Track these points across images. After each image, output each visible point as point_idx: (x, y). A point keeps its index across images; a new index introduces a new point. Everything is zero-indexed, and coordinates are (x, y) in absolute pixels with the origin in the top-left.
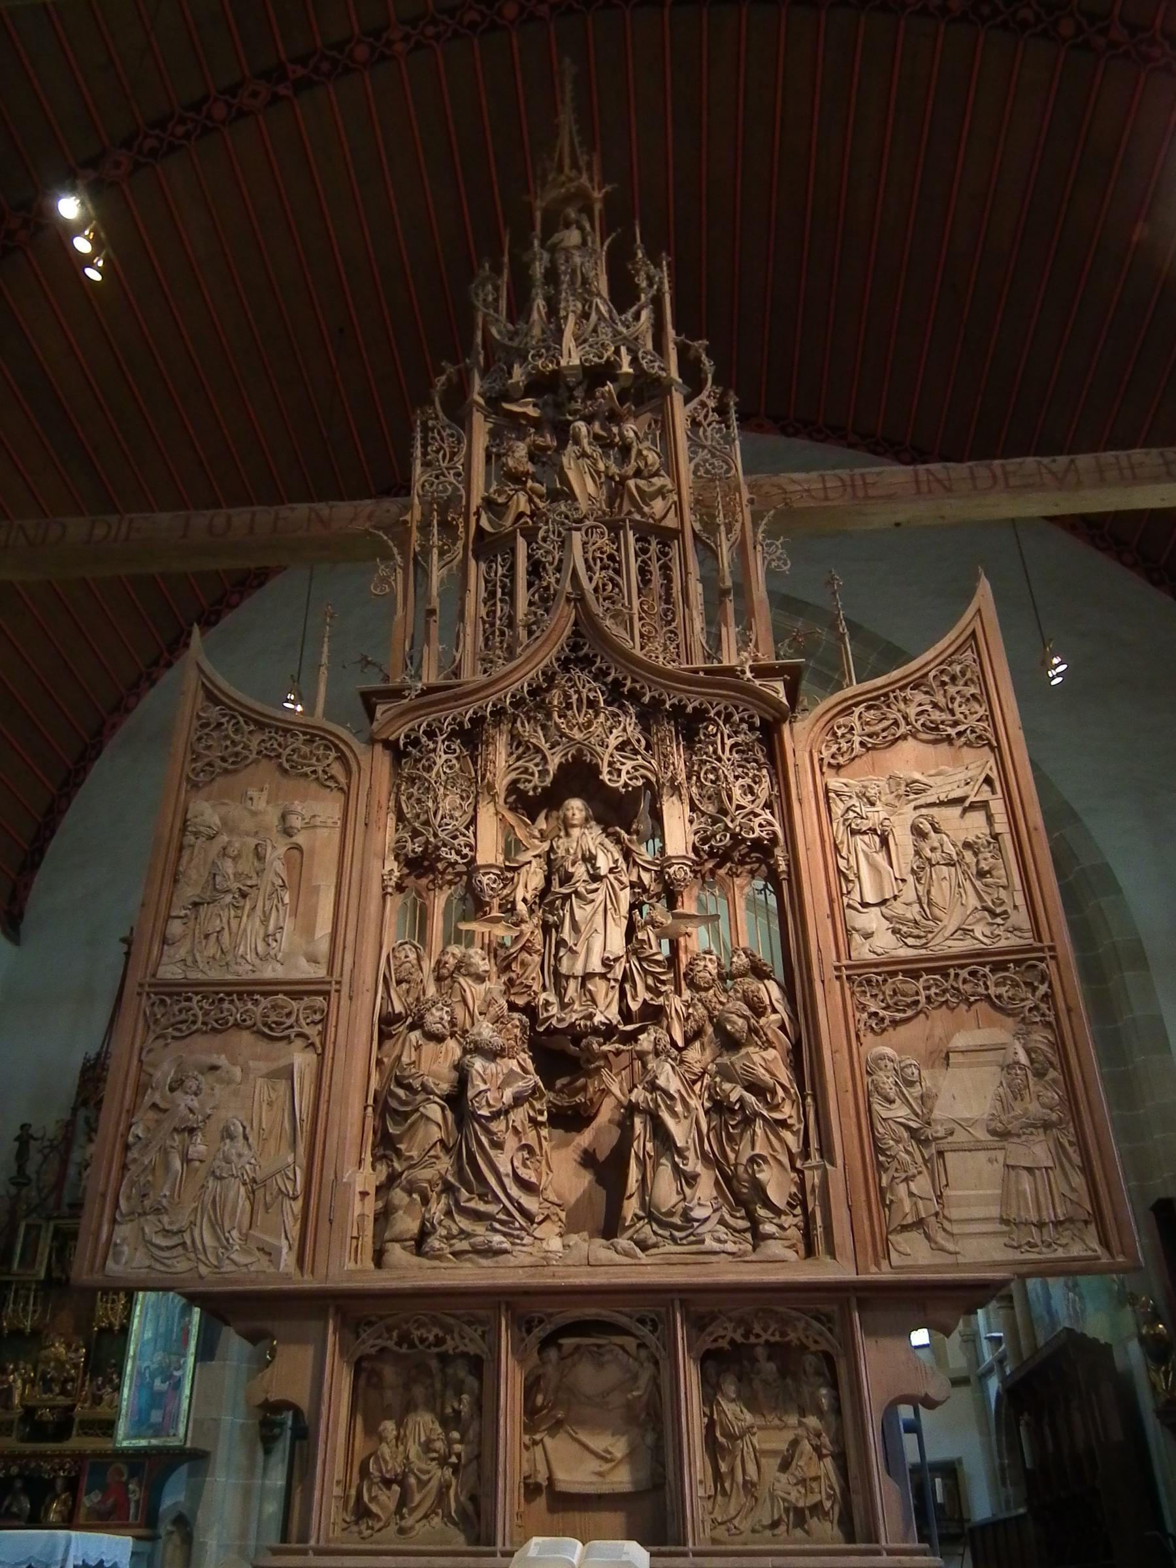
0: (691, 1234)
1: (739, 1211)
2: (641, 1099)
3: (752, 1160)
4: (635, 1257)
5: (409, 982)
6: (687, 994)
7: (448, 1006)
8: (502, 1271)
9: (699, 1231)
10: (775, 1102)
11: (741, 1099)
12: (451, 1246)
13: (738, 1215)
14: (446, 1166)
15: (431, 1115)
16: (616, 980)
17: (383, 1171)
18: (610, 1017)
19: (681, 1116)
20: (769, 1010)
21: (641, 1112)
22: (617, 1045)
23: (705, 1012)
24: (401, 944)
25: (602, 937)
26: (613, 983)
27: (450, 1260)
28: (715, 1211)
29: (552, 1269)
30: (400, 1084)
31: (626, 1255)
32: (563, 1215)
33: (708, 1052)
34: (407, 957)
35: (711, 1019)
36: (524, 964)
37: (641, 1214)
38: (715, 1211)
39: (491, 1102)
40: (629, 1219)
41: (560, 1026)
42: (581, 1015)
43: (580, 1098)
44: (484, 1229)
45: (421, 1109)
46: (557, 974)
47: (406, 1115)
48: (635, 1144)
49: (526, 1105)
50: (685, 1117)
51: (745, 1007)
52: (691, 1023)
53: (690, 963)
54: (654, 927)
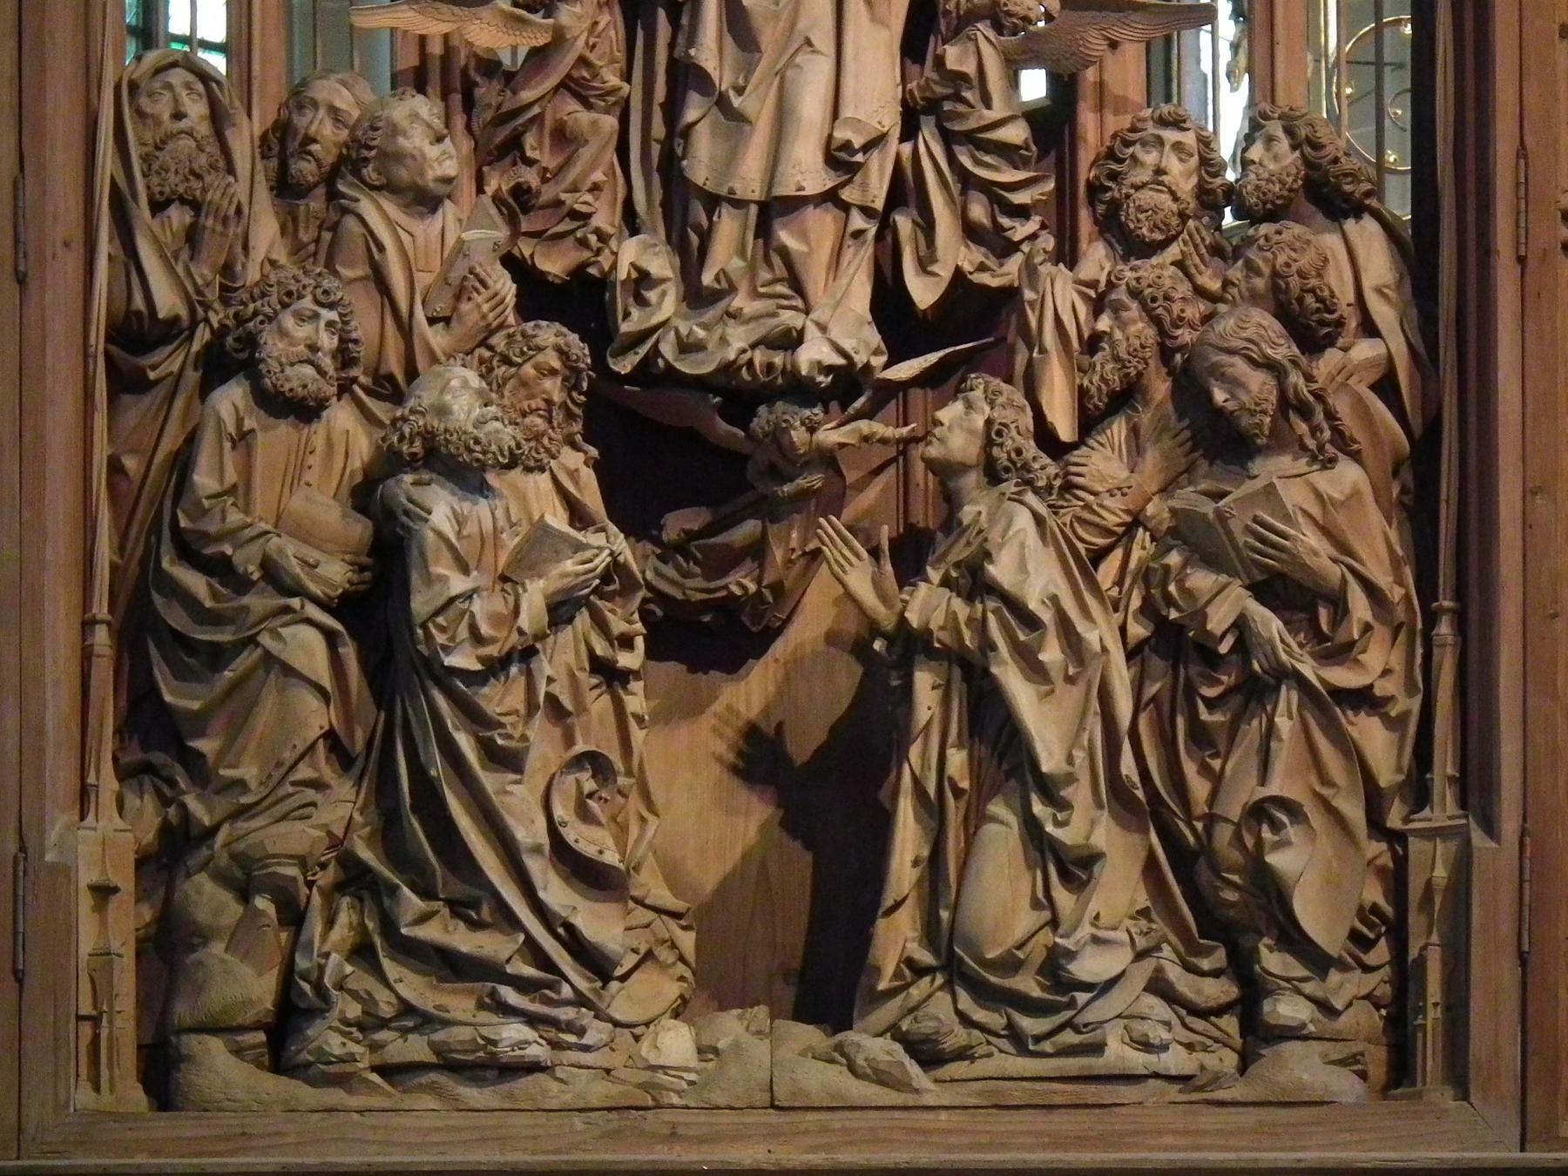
0: (1068, 1024)
1: (1207, 952)
2: (937, 620)
3: (1259, 812)
4: (903, 1085)
5: (195, 206)
6: (1096, 259)
7: (331, 306)
8: (525, 1119)
9: (1089, 1016)
10: (1341, 637)
11: (1241, 625)
12: (375, 1047)
13: (1205, 964)
14: (345, 810)
15: (298, 662)
16: (867, 212)
17: (147, 815)
18: (848, 345)
19: (1056, 675)
20: (1353, 324)
21: (932, 654)
22: (864, 426)
23: (1150, 333)
24: (159, 70)
25: (825, 66)
26: (858, 221)
27: (374, 1087)
28: (1140, 956)
29: (668, 1116)
30: (188, 552)
31: (881, 1082)
32: (687, 941)
33: (1151, 458)
34: (178, 115)
35: (1165, 354)
36: (563, 137)
37: (925, 957)
38: (1140, 956)
39: (485, 629)
40: (889, 969)
41: (686, 367)
42: (758, 331)
43: (741, 581)
44: (470, 1004)
45: (266, 640)
46: (670, 169)
47: (217, 656)
48: (914, 752)
49: (583, 619)
50: (1070, 680)
51: (1274, 326)
52: (1105, 369)
53: (1111, 155)
54: (999, 28)
